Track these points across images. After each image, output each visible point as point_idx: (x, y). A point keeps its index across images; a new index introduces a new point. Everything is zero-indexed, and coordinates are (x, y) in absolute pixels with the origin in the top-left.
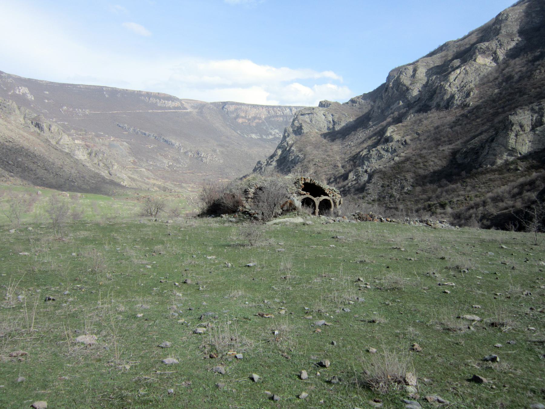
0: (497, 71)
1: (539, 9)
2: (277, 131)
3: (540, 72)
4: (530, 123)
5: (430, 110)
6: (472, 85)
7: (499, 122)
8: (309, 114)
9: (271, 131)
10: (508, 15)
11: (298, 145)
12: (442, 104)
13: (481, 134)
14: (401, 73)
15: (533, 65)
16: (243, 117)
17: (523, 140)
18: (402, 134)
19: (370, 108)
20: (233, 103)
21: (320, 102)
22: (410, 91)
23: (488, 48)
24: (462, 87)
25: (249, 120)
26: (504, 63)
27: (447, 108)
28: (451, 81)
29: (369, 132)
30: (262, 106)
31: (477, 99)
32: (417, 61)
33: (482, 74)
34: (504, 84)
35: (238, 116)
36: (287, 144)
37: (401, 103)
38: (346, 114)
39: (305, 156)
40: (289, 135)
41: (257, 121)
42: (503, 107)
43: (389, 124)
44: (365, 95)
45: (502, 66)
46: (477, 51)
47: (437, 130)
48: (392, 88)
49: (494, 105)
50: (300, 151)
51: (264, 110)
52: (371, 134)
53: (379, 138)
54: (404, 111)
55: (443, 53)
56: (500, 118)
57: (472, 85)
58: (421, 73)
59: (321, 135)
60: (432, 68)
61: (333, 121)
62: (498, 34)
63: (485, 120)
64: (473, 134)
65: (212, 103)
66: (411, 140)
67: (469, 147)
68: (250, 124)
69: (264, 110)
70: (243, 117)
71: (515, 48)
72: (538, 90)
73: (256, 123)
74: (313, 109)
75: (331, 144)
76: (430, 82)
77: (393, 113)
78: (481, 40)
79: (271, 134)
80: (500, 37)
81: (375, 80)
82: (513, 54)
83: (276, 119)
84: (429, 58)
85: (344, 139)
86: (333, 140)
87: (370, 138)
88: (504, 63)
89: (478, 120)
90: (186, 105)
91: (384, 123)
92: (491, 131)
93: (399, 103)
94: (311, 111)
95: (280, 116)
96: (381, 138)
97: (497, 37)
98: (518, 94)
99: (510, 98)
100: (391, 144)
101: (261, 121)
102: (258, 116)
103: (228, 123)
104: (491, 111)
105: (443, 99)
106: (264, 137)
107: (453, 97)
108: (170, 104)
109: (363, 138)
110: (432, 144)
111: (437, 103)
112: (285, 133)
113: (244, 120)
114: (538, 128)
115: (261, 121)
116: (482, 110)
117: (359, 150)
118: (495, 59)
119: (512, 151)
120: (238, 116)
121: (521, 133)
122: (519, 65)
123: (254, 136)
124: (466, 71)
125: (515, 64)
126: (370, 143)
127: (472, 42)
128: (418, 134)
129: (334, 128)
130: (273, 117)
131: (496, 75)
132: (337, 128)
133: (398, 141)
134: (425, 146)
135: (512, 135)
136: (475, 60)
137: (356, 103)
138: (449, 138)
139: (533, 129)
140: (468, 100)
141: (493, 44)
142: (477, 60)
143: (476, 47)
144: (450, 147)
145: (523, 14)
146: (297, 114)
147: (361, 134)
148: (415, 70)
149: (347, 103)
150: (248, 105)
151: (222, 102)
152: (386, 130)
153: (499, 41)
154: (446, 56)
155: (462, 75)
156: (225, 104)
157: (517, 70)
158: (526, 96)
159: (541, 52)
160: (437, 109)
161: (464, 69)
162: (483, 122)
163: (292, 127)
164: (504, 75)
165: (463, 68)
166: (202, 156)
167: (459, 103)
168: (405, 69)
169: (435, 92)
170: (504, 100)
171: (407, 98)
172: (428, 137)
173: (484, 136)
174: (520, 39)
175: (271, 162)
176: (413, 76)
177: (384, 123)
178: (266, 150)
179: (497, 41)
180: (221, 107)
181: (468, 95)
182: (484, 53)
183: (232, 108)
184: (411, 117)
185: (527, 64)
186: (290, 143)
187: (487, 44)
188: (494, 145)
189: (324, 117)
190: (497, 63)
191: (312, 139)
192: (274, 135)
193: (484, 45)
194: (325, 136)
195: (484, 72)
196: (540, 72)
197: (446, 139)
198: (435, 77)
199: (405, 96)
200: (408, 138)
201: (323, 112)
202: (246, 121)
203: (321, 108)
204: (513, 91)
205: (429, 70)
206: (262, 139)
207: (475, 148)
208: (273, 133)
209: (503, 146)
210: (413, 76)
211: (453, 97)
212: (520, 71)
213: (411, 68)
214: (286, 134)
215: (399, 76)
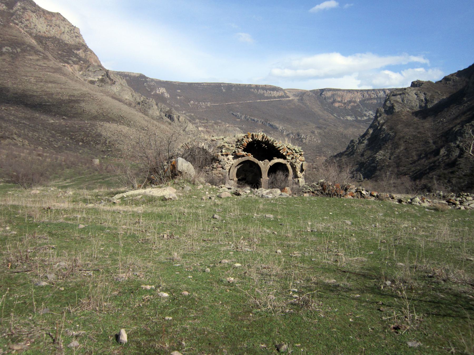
2: (371, 112)
8: (400, 94)
9: (365, 113)
11: (389, 124)
16: (339, 102)
20: (330, 90)
21: (413, 83)
25: (345, 104)
30: (357, 91)
36: (379, 123)
39: (396, 133)
40: (380, 115)
41: (352, 104)
44: (459, 72)
50: (391, 129)
51: (359, 94)
59: (413, 113)
61: (425, 99)
65: (311, 91)
68: (345, 107)
69: (359, 94)
70: (339, 102)
73: (352, 106)
74: (405, 89)
75: (422, 121)
79: (365, 115)
83: (371, 101)
87: (464, 113)
90: (288, 94)
94: (403, 92)
95: (374, 99)
101: (356, 104)
102: (354, 100)
103: (325, 108)
106: (359, 118)
108: (275, 94)
112: (376, 114)
113: (340, 104)
115: (356, 104)
117: (451, 126)
120: (334, 101)
123: (349, 118)
126: (463, 118)
129: (426, 106)
130: (368, 99)
132: (430, 106)
137: (450, 81)
146: (389, 95)
147: (454, 111)
149: (441, 81)
150: (344, 90)
151: (320, 90)
156: (322, 90)
166: (302, 137)
175: (363, 140)
178: (361, 130)
180: (319, 94)
183: (329, 94)
186: (381, 122)
189: (416, 96)
191: (403, 117)
192: (369, 116)
194: (416, 114)
201: (415, 92)
202: (342, 105)
203: (413, 88)
206: (357, 121)
208: (368, 114)
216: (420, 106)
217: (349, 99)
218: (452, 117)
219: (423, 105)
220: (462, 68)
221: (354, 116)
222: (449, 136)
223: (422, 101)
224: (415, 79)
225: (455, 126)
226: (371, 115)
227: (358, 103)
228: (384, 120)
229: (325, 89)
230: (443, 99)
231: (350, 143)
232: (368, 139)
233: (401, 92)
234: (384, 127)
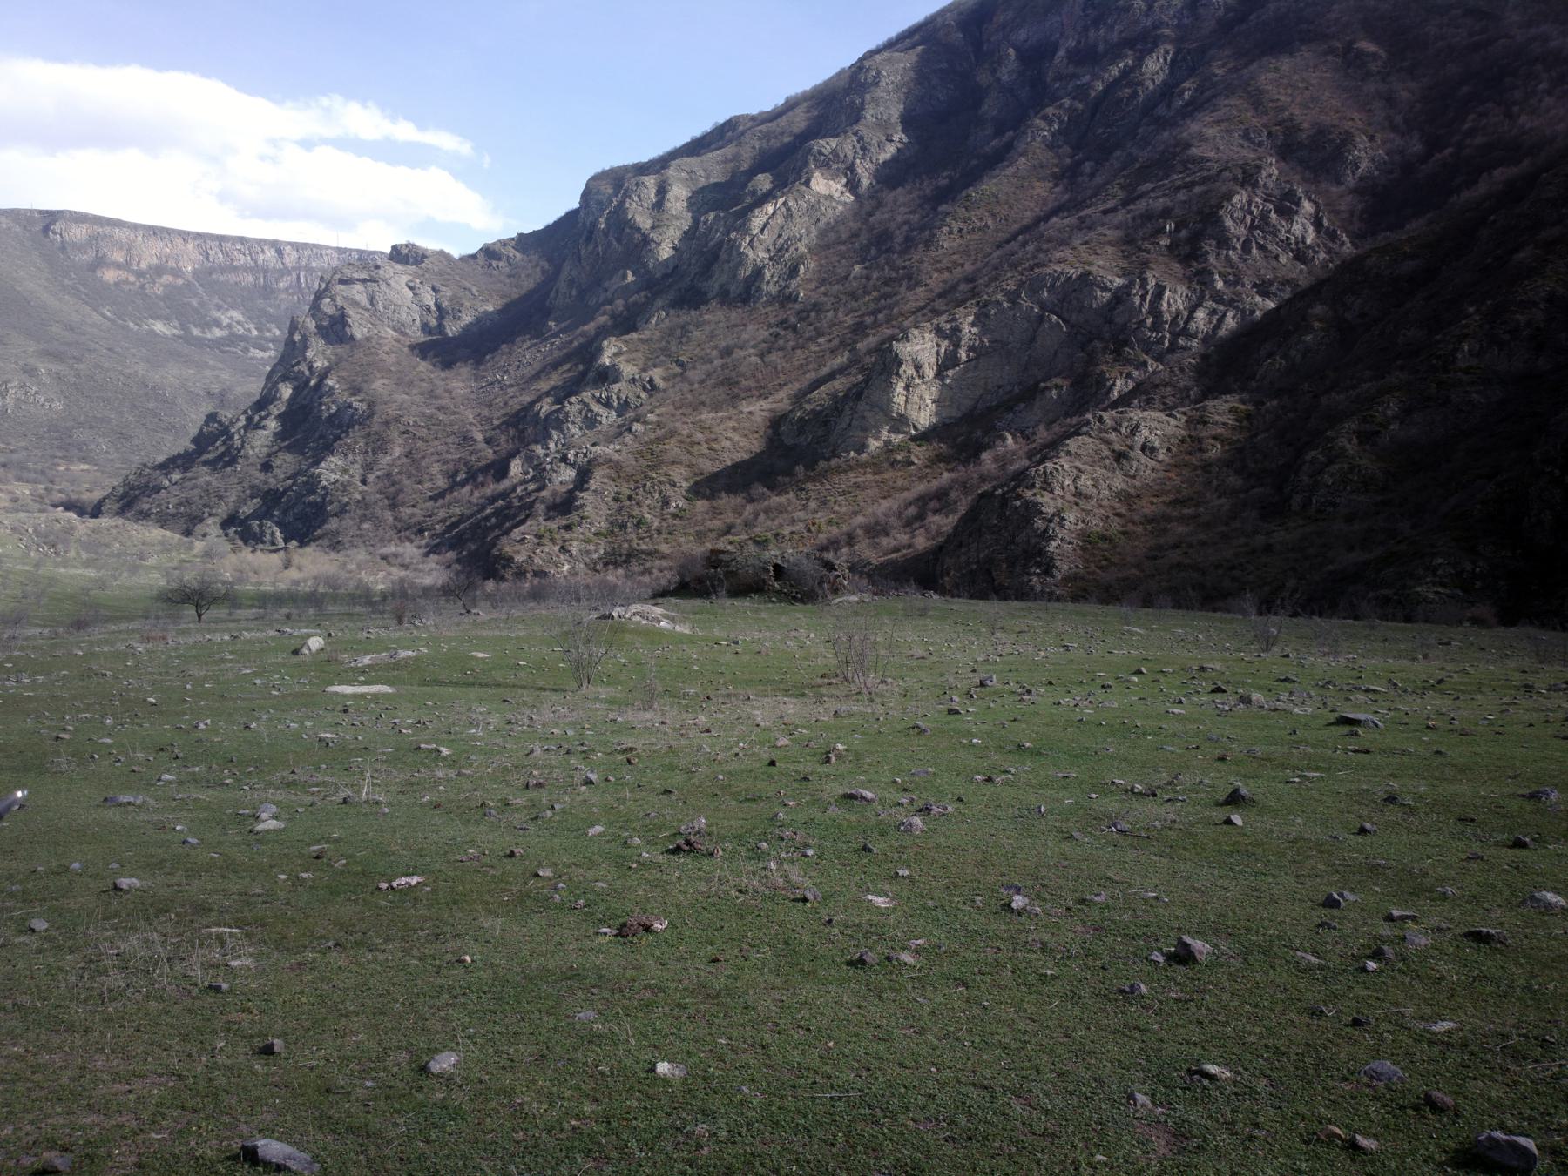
0: (855, 214)
1: (945, 65)
2: (237, 315)
3: (951, 233)
4: (933, 360)
5: (706, 303)
6: (803, 249)
7: (870, 352)
8: (364, 281)
9: (217, 314)
10: (878, 73)
11: (345, 374)
12: (734, 290)
13: (831, 376)
14: (627, 195)
15: (935, 209)
16: (118, 266)
17: (921, 398)
18: (641, 363)
19: (538, 277)
21: (394, 248)
22: (653, 245)
23: (835, 152)
24: (780, 250)
25: (140, 274)
26: (872, 197)
27: (745, 301)
28: (755, 232)
29: (551, 348)
30: (185, 235)
31: (813, 285)
32: (662, 163)
33: (823, 220)
34: (873, 251)
35: (100, 262)
36: (311, 368)
37: (630, 277)
38: (474, 289)
39: (371, 405)
41: (167, 279)
42: (874, 313)
43: (603, 333)
44: (521, 237)
45: (867, 203)
47: (729, 360)
48: (606, 233)
49: (855, 304)
50: (355, 391)
51: (190, 246)
52: (557, 354)
53: (581, 367)
54: (640, 298)
55: (729, 151)
56: (872, 341)
57: (803, 249)
58: (677, 199)
59: (412, 347)
60: (702, 189)
62: (857, 121)
63: (836, 342)
64: (811, 376)
66: (664, 379)
67: (808, 407)
68: (142, 287)
69: (190, 246)
70: (118, 266)
71: (894, 159)
72: (946, 275)
73: (166, 286)
74: (377, 267)
75: (443, 375)
76: (702, 228)
77: (610, 302)
78: (819, 128)
80: (860, 127)
81: (550, 201)
82: (891, 176)
83: (233, 278)
84: (691, 162)
85: (479, 362)
86: (448, 365)
87: (555, 366)
88: (872, 197)
89: (821, 340)
91: (590, 328)
92: (854, 371)
93: (625, 277)
96: (586, 371)
97: (856, 128)
98: (905, 283)
99: (888, 289)
100: (616, 387)
101: (180, 281)
102: (172, 264)
104: (849, 320)
105: (735, 276)
106: (196, 332)
107: (758, 273)
109: (537, 366)
110: (720, 393)
111: (721, 286)
112: (291, 333)
113: (123, 275)
114: (950, 373)
115: (180, 281)
116: (830, 314)
117: (528, 399)
118: (852, 185)
119: (899, 423)
120: (100, 262)
121: (917, 381)
122: (904, 204)
123: (159, 327)
124: (789, 209)
125: (895, 202)
126: (555, 379)
127: (796, 130)
128: (681, 365)
129: (440, 326)
130: (223, 270)
131: (854, 226)
132: (452, 329)
133: (633, 380)
134: (703, 398)
135: (900, 388)
136: (807, 183)
137: (499, 259)
138: (758, 381)
139: (939, 375)
140: (793, 284)
141: (848, 146)
142: (813, 184)
144: (766, 405)
145: (912, 74)
146: (327, 277)
147: (527, 354)
148: (662, 191)
149: (474, 257)
150: (135, 227)
152: (600, 350)
153: (861, 139)
154: (736, 158)
155: (779, 220)
157: (899, 219)
158: (920, 290)
159: (950, 177)
160: (722, 303)
161: (784, 204)
162: (831, 345)
163: (314, 317)
164: (872, 229)
165: (781, 201)
167: (773, 289)
168: (637, 184)
169: (716, 257)
170: (875, 294)
171: (645, 265)
172: (709, 375)
173: (839, 385)
174: (905, 139)
175: (262, 419)
176: (659, 205)
177: (590, 328)
178: (208, 373)
181: (793, 271)
182: (826, 165)
184: (659, 321)
185: (921, 206)
186: (319, 364)
187: (833, 143)
188: (862, 406)
189: (410, 294)
190: (857, 195)
191: (385, 357)
192: (229, 326)
193: (828, 145)
194: (422, 350)
195: (828, 216)
196: (951, 233)
197: (752, 383)
198: (712, 215)
199: (639, 258)
200: (657, 374)
201: (405, 278)
202: (132, 279)
203: (399, 267)
204: (894, 275)
205: (695, 194)
206: (187, 338)
207: (820, 412)
208: (225, 321)
209: (882, 410)
211: (758, 273)
212: (905, 223)
213: (650, 181)
214: (297, 337)
215: (622, 203)
216: (425, 327)
217: (155, 261)
218: (527, 371)
219: (433, 323)
220: (527, 231)
221: (176, 323)
222: (525, 427)
223: (429, 310)
224: (401, 240)
225: (539, 399)
226: (239, 323)
227: (189, 277)
228: (328, 359)
229: (59, 212)
230: (486, 312)
231: (206, 423)
232: (279, 417)
233: (364, 275)
234: (330, 382)
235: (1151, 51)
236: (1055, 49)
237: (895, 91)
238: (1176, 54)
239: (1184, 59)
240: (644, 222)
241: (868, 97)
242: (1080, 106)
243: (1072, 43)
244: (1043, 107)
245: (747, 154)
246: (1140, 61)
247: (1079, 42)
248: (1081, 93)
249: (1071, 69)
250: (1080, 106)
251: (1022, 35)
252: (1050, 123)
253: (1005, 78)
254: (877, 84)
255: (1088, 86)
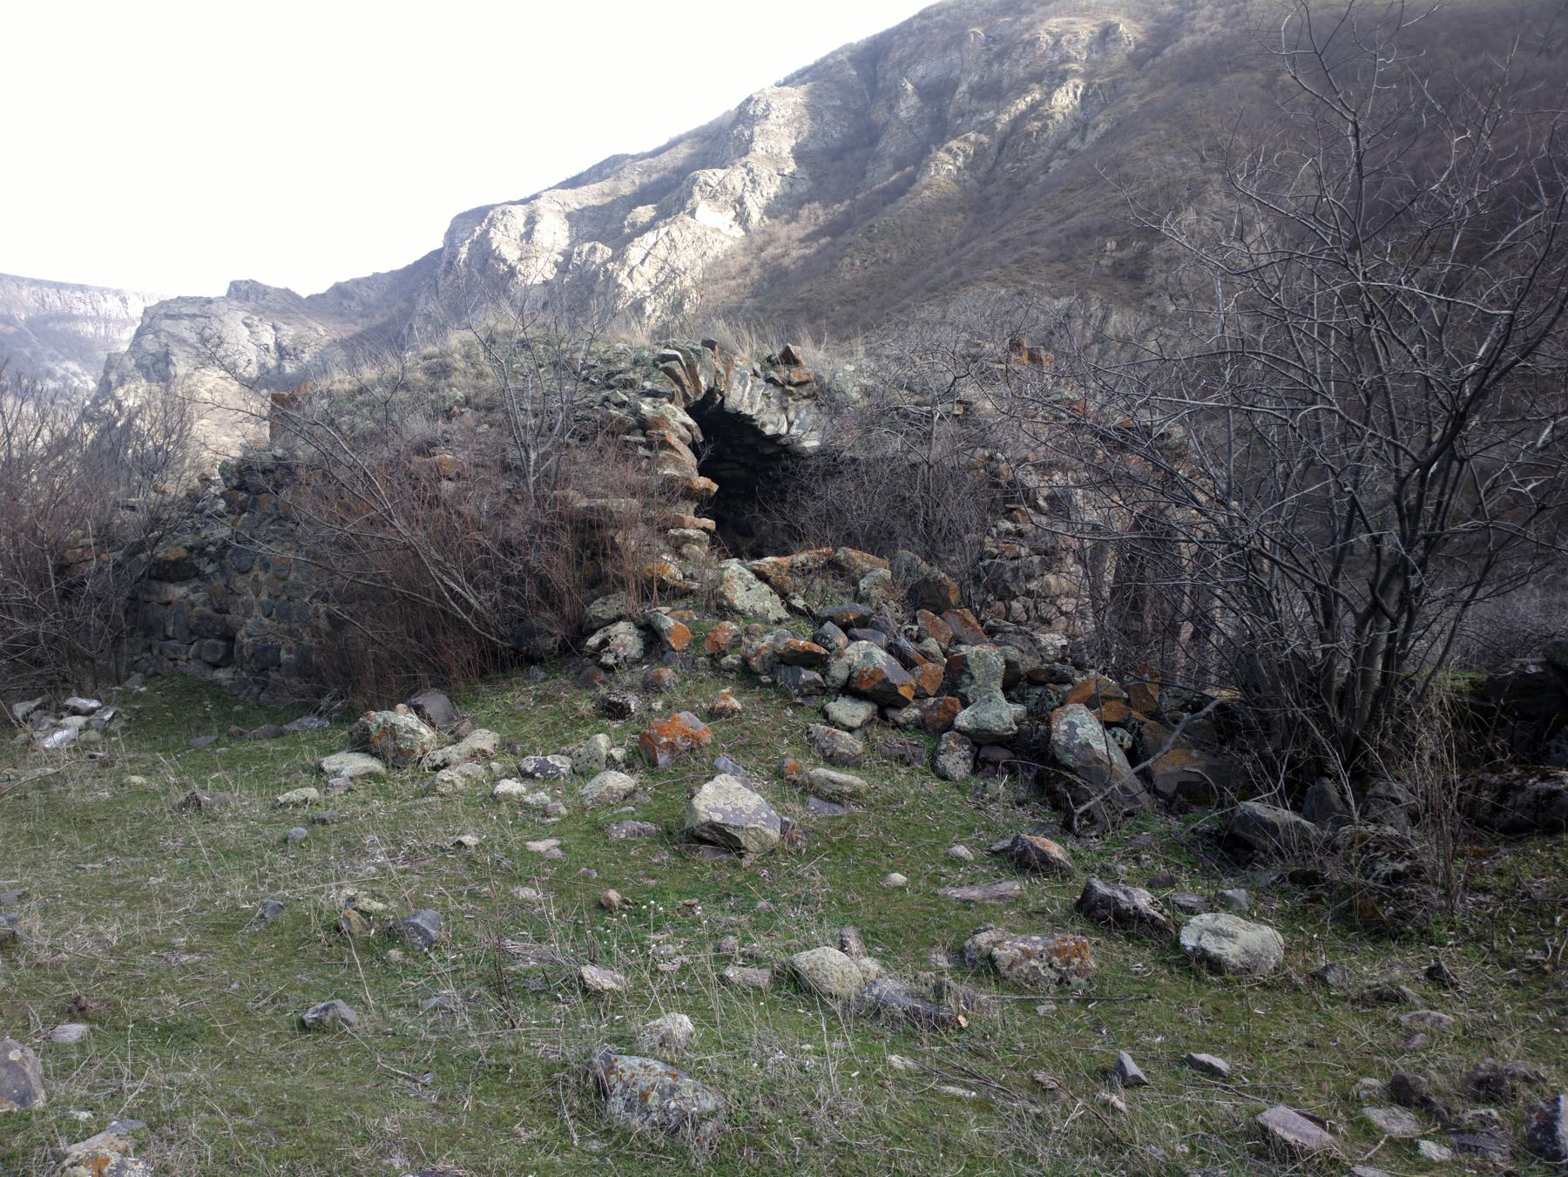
9: (51, 365)
10: (768, 105)
32: (536, 197)
33: (711, 254)
46: (696, 189)
55: (606, 185)
62: (746, 153)
84: (568, 192)
97: (744, 160)
118: (742, 218)
131: (745, 261)
136: (692, 213)
141: (735, 178)
143: (695, 180)
148: (531, 221)
153: (751, 170)
155: (661, 251)
165: (663, 231)
168: (504, 213)
176: (528, 236)
179: (744, 170)
182: (714, 197)
187: (720, 173)
190: (746, 230)
192: (64, 378)
193: (712, 176)
195: (717, 249)
208: (60, 372)
210: (528, 236)
213: (520, 213)
215: (487, 232)
226: (75, 374)
235: (1059, 86)
236: (956, 85)
237: (786, 125)
238: (1086, 89)
239: (1095, 94)
240: (510, 253)
241: (757, 129)
242: (984, 138)
243: (975, 78)
244: (944, 143)
245: (627, 185)
246: (1048, 96)
247: (982, 77)
248: (988, 127)
249: (974, 103)
250: (984, 138)
251: (920, 70)
252: (955, 157)
253: (903, 114)
254: (766, 117)
255: (995, 120)
